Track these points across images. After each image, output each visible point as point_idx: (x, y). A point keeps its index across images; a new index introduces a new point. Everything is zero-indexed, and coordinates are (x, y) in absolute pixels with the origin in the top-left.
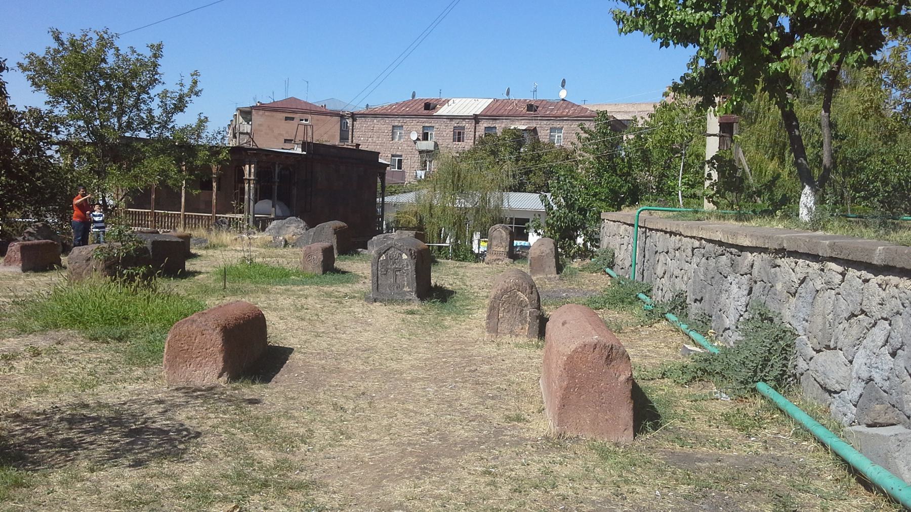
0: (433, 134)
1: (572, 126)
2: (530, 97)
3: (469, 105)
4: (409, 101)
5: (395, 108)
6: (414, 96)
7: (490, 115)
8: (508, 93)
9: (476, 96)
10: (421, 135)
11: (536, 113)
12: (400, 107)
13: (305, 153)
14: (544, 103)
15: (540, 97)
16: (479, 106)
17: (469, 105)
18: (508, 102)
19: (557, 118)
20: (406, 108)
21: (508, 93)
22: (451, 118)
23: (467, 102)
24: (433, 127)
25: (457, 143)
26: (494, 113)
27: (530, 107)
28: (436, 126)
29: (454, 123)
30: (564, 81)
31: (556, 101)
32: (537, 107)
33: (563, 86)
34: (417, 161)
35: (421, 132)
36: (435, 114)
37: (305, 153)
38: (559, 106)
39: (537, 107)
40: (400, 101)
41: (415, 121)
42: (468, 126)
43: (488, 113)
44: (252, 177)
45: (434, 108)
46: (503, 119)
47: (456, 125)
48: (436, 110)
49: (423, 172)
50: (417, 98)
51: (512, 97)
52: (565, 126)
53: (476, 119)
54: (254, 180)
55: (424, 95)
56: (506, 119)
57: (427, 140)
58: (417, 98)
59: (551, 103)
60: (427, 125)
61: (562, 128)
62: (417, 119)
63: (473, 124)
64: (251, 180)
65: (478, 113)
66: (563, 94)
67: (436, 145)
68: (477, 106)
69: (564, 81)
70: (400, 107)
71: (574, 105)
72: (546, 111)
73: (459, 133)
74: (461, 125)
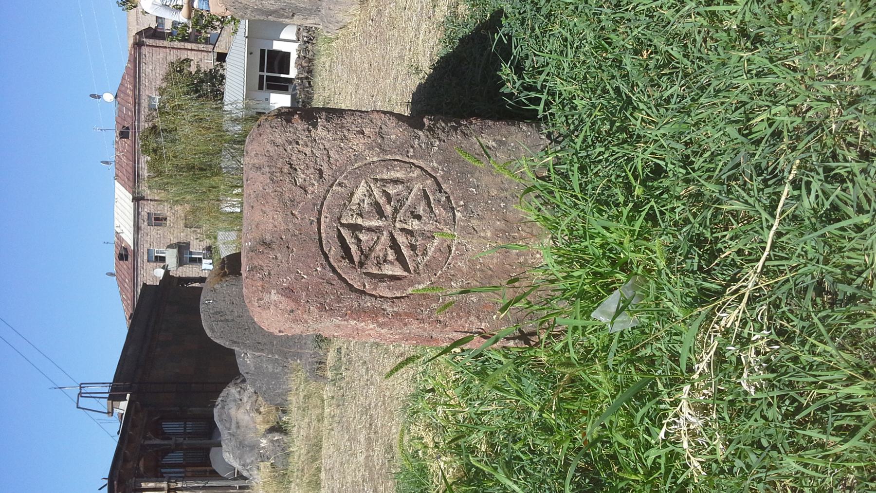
0: (158, 250)
1: (147, 84)
2: (114, 135)
3: (122, 208)
4: (117, 279)
5: (126, 295)
6: (112, 274)
7: (133, 181)
8: (107, 163)
9: (111, 200)
10: (159, 264)
11: (130, 129)
12: (124, 290)
13: (128, 395)
14: (119, 120)
15: (113, 124)
16: (123, 197)
17: (122, 208)
18: (118, 163)
19: (137, 102)
20: (125, 282)
21: (107, 163)
22: (137, 228)
23: (119, 211)
24: (148, 250)
25: (168, 222)
26: (131, 178)
27: (124, 134)
28: (147, 246)
29: (144, 225)
30: (93, 96)
31: (118, 106)
32: (124, 127)
33: (99, 97)
34: (191, 269)
35: (155, 264)
36: (132, 248)
37: (128, 395)
38: (123, 102)
39: (124, 127)
40: (117, 290)
41: (141, 272)
42: (147, 208)
43: (131, 184)
44: (164, 485)
45: (126, 249)
46: (138, 167)
47: (146, 223)
48: (128, 247)
49: (204, 261)
50: (114, 271)
51: (112, 158)
52: (147, 93)
53: (138, 199)
54: (169, 482)
55: (111, 262)
56: (138, 164)
57: (164, 258)
58: (114, 271)
59: (120, 110)
60: (146, 257)
61: (150, 97)
62: (139, 268)
63: (145, 202)
64: (169, 486)
65: (131, 197)
66: (109, 97)
67: (170, 246)
68: (123, 198)
69: (91, 96)
70: (124, 290)
71: (122, 84)
72: (128, 116)
73: (157, 219)
74: (146, 217)
